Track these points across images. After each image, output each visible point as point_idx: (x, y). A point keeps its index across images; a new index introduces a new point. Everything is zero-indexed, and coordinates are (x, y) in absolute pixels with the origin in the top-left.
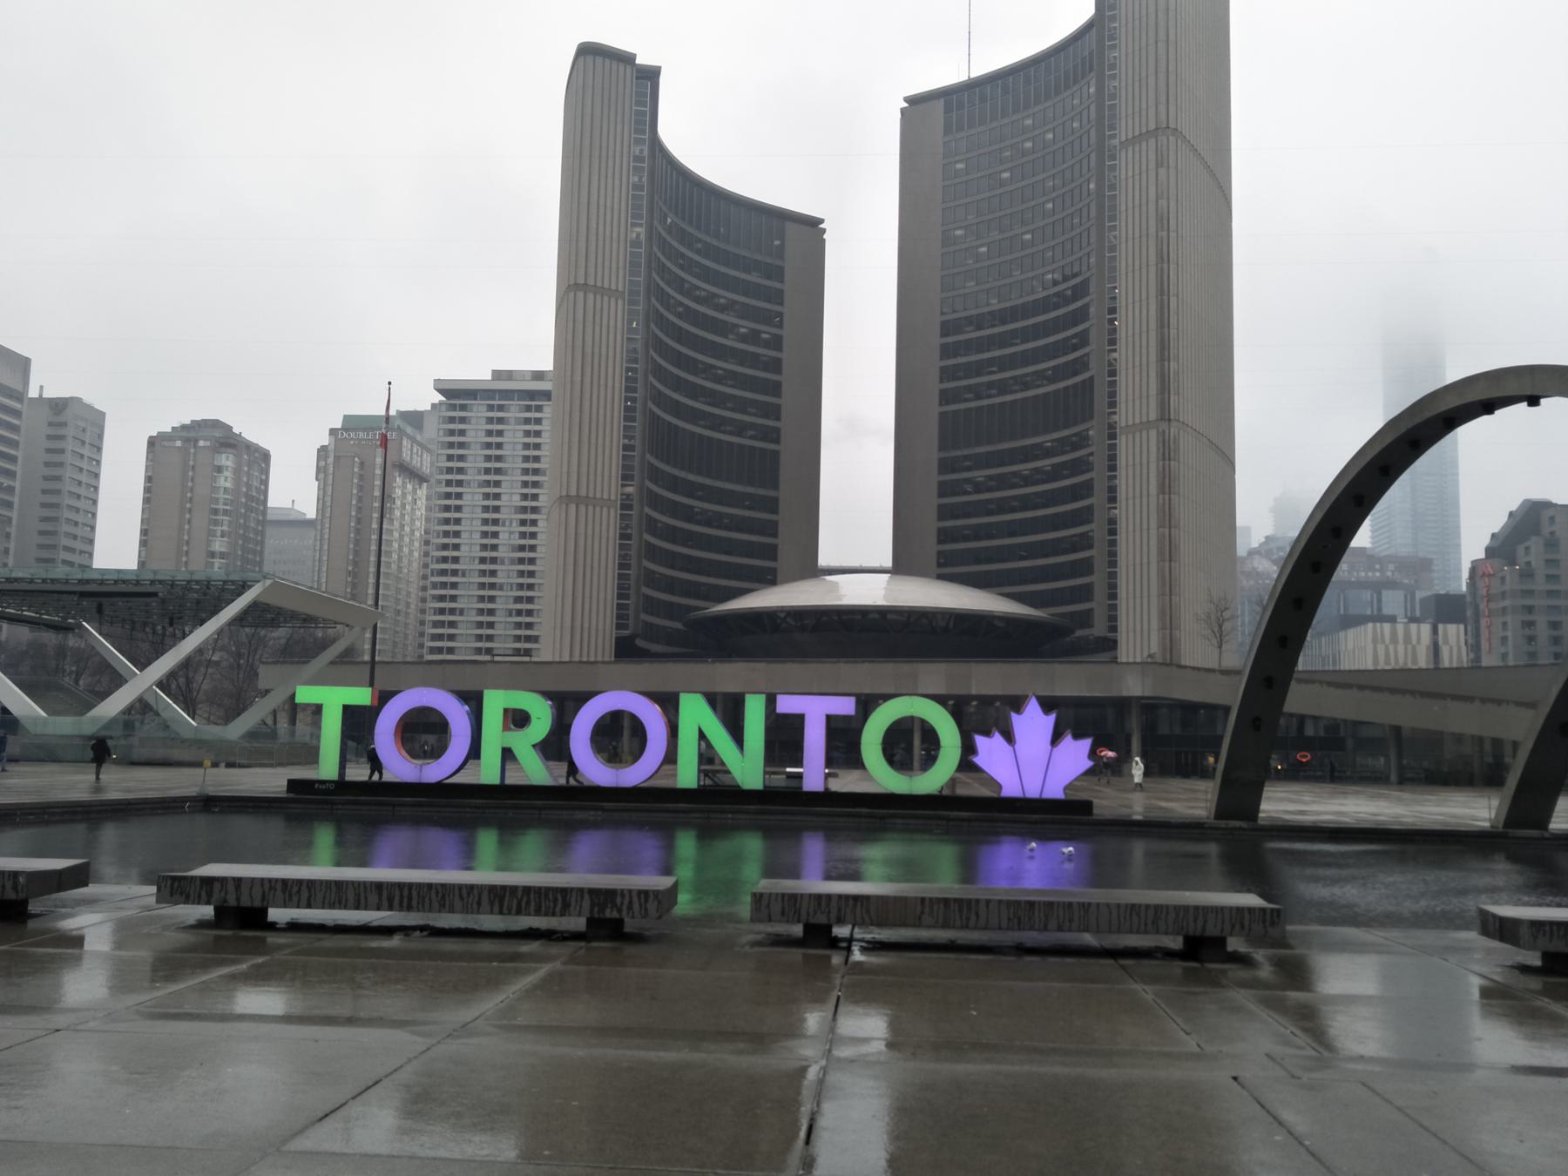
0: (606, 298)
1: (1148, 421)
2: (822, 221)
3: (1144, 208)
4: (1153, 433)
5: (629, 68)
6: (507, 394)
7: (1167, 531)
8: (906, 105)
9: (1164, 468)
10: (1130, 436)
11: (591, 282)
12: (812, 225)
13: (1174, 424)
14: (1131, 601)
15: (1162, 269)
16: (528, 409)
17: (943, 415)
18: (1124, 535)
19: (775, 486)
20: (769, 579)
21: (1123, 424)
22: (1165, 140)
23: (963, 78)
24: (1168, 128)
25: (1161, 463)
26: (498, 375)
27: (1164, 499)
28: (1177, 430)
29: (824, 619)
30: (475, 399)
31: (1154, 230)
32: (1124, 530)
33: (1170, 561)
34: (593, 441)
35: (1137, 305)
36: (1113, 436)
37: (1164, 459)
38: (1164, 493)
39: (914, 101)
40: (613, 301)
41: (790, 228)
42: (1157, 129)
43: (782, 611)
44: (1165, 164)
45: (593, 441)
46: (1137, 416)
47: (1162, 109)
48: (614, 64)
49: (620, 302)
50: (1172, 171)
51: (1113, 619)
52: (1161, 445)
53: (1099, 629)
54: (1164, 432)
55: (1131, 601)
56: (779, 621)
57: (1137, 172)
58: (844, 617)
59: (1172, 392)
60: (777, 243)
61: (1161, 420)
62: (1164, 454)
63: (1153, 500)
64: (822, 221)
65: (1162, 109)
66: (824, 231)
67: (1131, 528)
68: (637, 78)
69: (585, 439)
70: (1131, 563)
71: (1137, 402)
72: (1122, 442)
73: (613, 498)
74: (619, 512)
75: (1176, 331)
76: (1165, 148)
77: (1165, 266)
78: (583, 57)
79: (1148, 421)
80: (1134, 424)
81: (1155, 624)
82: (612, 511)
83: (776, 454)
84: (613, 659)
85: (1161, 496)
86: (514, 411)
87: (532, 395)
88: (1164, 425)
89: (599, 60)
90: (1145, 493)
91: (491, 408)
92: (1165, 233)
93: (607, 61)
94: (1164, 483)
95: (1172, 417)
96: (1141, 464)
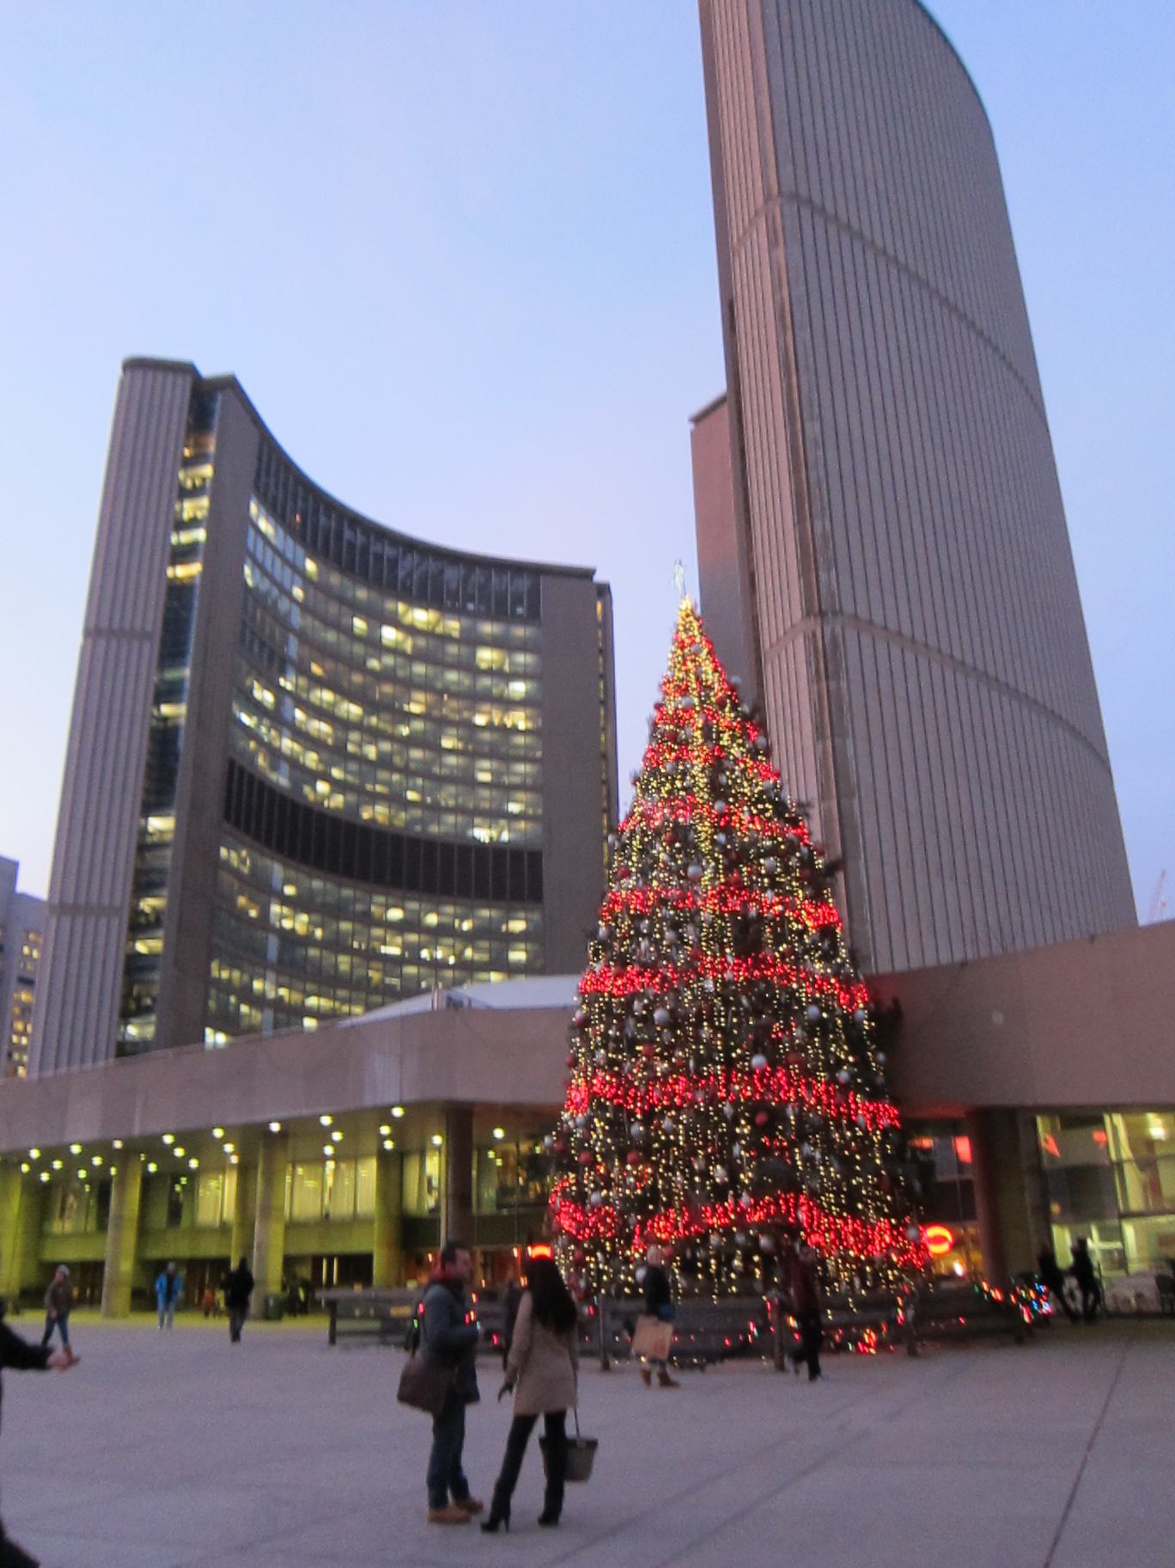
15: (789, 386)
27: (824, 751)
28: (838, 630)
37: (819, 680)
40: (136, 644)
54: (814, 635)
62: (817, 670)
75: (822, 473)
82: (115, 922)
85: (820, 746)
89: (139, 374)
94: (822, 721)
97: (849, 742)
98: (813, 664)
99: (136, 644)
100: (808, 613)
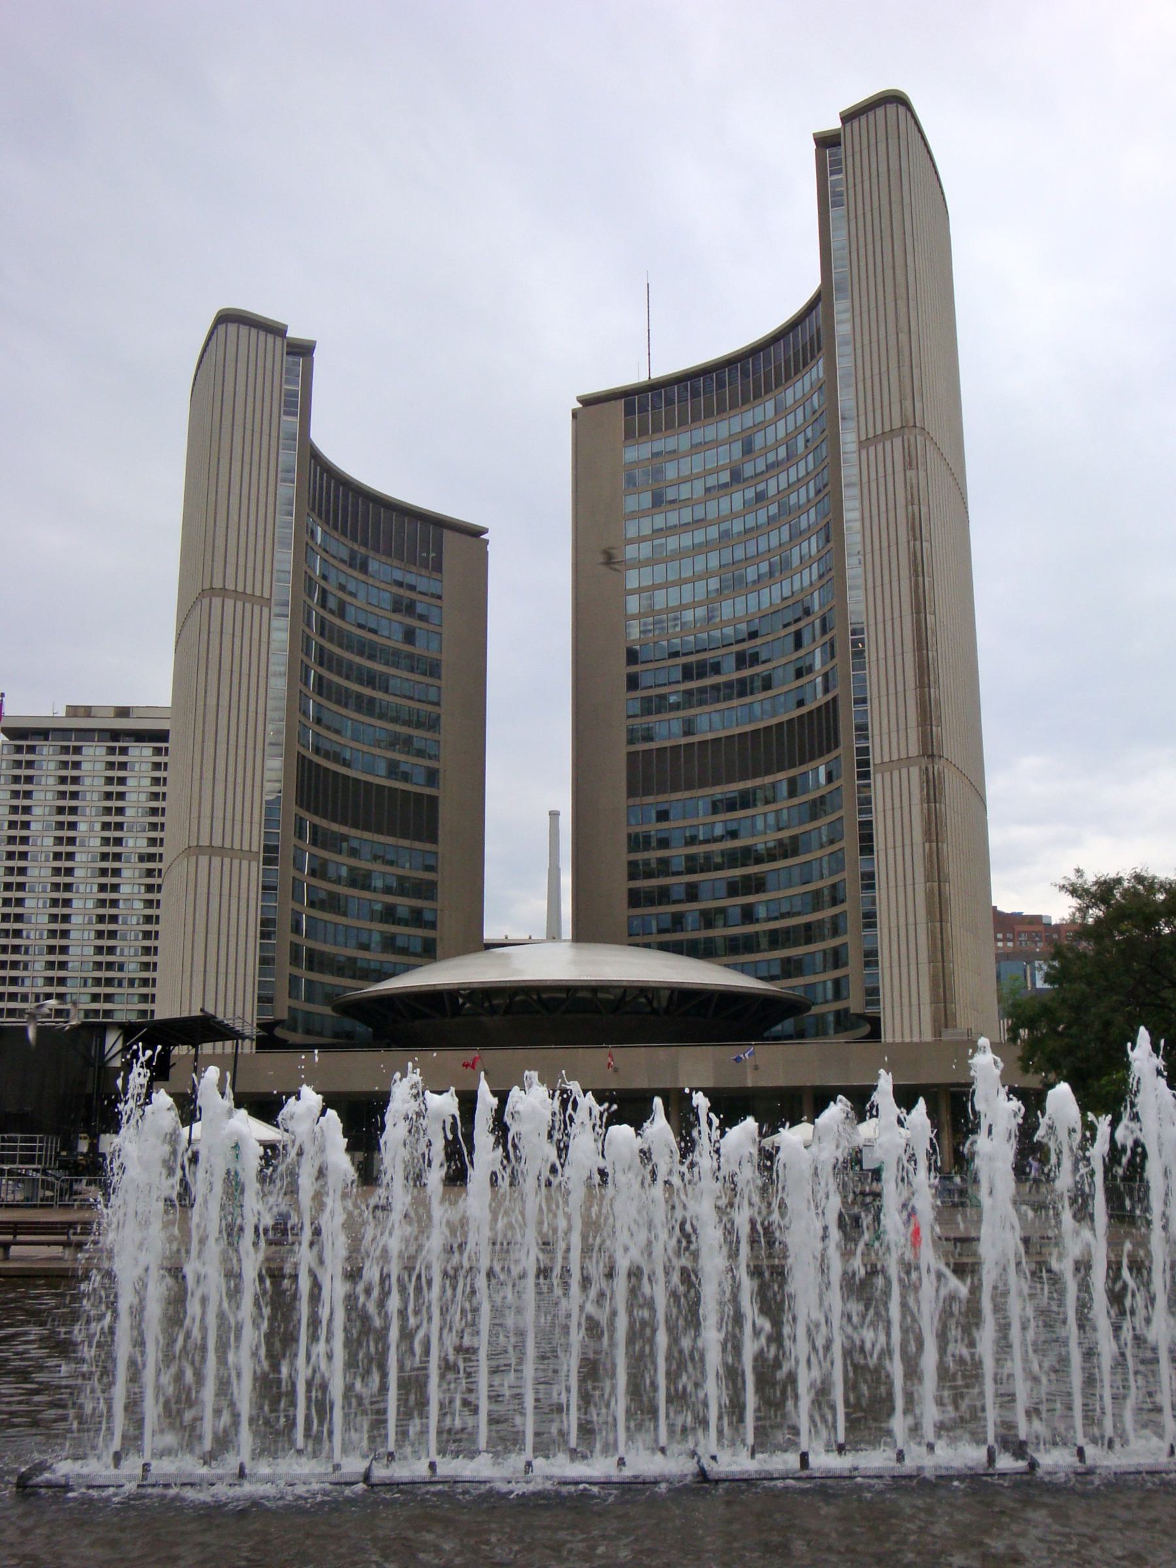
0: (248, 606)
1: (908, 758)
2: (484, 531)
3: (891, 514)
4: (915, 772)
5: (279, 340)
6: (86, 734)
7: (936, 884)
8: (579, 405)
9: (929, 810)
10: (887, 775)
11: (230, 586)
12: (475, 533)
13: (936, 760)
14: (896, 970)
16: (111, 751)
17: (632, 756)
18: (884, 892)
19: (433, 838)
20: (429, 953)
21: (878, 761)
23: (643, 378)
24: (915, 426)
25: (925, 805)
26: (73, 711)
29: (518, 998)
30: (46, 739)
31: (905, 540)
32: (883, 885)
33: (941, 921)
34: (231, 779)
35: (889, 624)
36: (865, 775)
37: (928, 802)
38: (931, 841)
39: (589, 402)
40: (257, 608)
41: (448, 535)
42: (902, 427)
43: (465, 989)
45: (231, 779)
46: (894, 750)
47: (908, 404)
48: (262, 335)
49: (266, 610)
50: (922, 474)
51: (873, 994)
53: (855, 1003)
54: (927, 769)
55: (896, 970)
56: (461, 1001)
57: (881, 474)
58: (544, 996)
60: (432, 555)
61: (923, 755)
62: (928, 794)
63: (918, 850)
64: (484, 531)
65: (908, 404)
66: (486, 542)
67: (892, 884)
68: (288, 353)
69: (220, 776)
70: (894, 924)
71: (894, 735)
72: (878, 783)
73: (255, 849)
74: (261, 867)
76: (913, 448)
78: (224, 326)
79: (908, 758)
80: (891, 761)
81: (926, 996)
82: (254, 864)
83: (433, 801)
84: (254, 1051)
85: (927, 845)
86: (94, 756)
87: (115, 735)
88: (925, 762)
89: (244, 330)
90: (907, 842)
91: (65, 750)
92: (918, 543)
93: (254, 331)
94: (930, 829)
96: (901, 808)
99: (257, 608)
100: (923, 755)
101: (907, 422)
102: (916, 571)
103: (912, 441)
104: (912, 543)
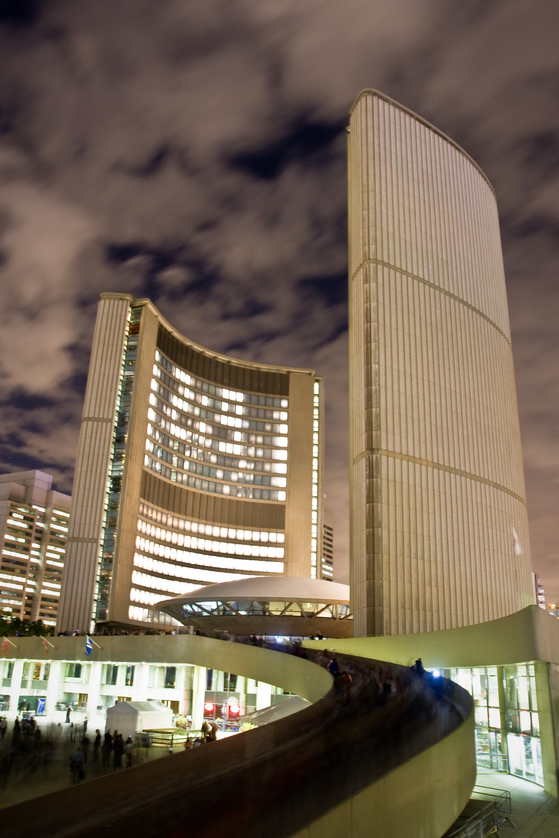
1: (362, 452)
13: (375, 451)
22: (368, 266)
24: (369, 259)
25: (368, 480)
27: (369, 506)
37: (369, 479)
44: (368, 281)
52: (368, 468)
54: (369, 457)
59: (374, 429)
77: (369, 344)
85: (368, 505)
92: (369, 324)
94: (369, 495)
95: (374, 447)
97: (379, 504)
98: (368, 471)
101: (366, 257)
102: (367, 340)
103: (368, 266)
104: (366, 325)
